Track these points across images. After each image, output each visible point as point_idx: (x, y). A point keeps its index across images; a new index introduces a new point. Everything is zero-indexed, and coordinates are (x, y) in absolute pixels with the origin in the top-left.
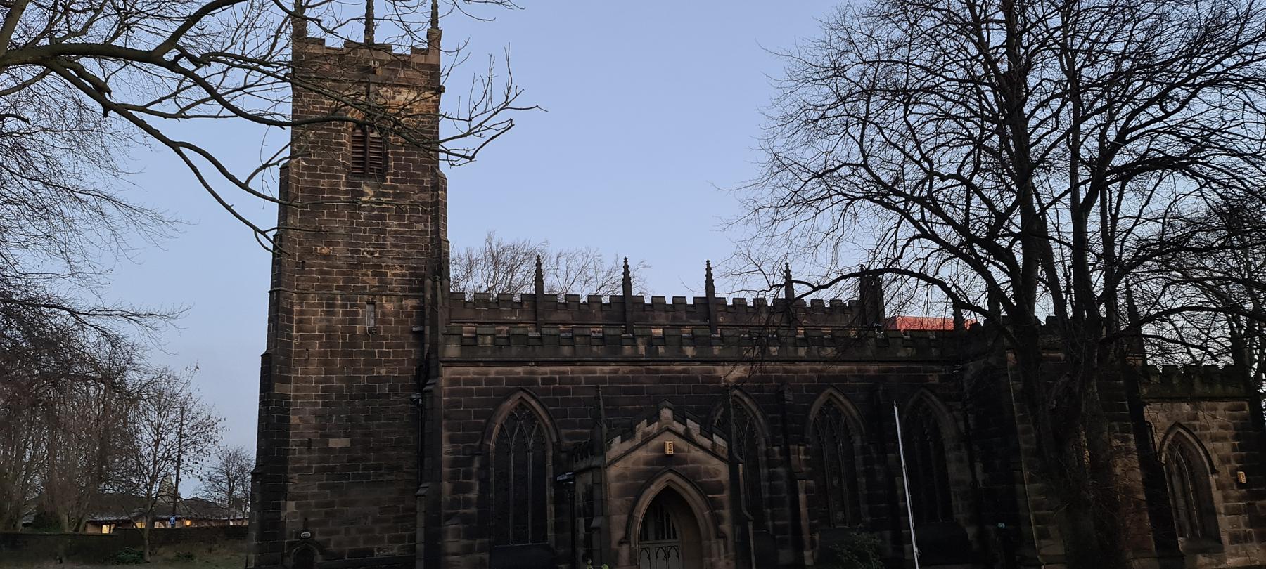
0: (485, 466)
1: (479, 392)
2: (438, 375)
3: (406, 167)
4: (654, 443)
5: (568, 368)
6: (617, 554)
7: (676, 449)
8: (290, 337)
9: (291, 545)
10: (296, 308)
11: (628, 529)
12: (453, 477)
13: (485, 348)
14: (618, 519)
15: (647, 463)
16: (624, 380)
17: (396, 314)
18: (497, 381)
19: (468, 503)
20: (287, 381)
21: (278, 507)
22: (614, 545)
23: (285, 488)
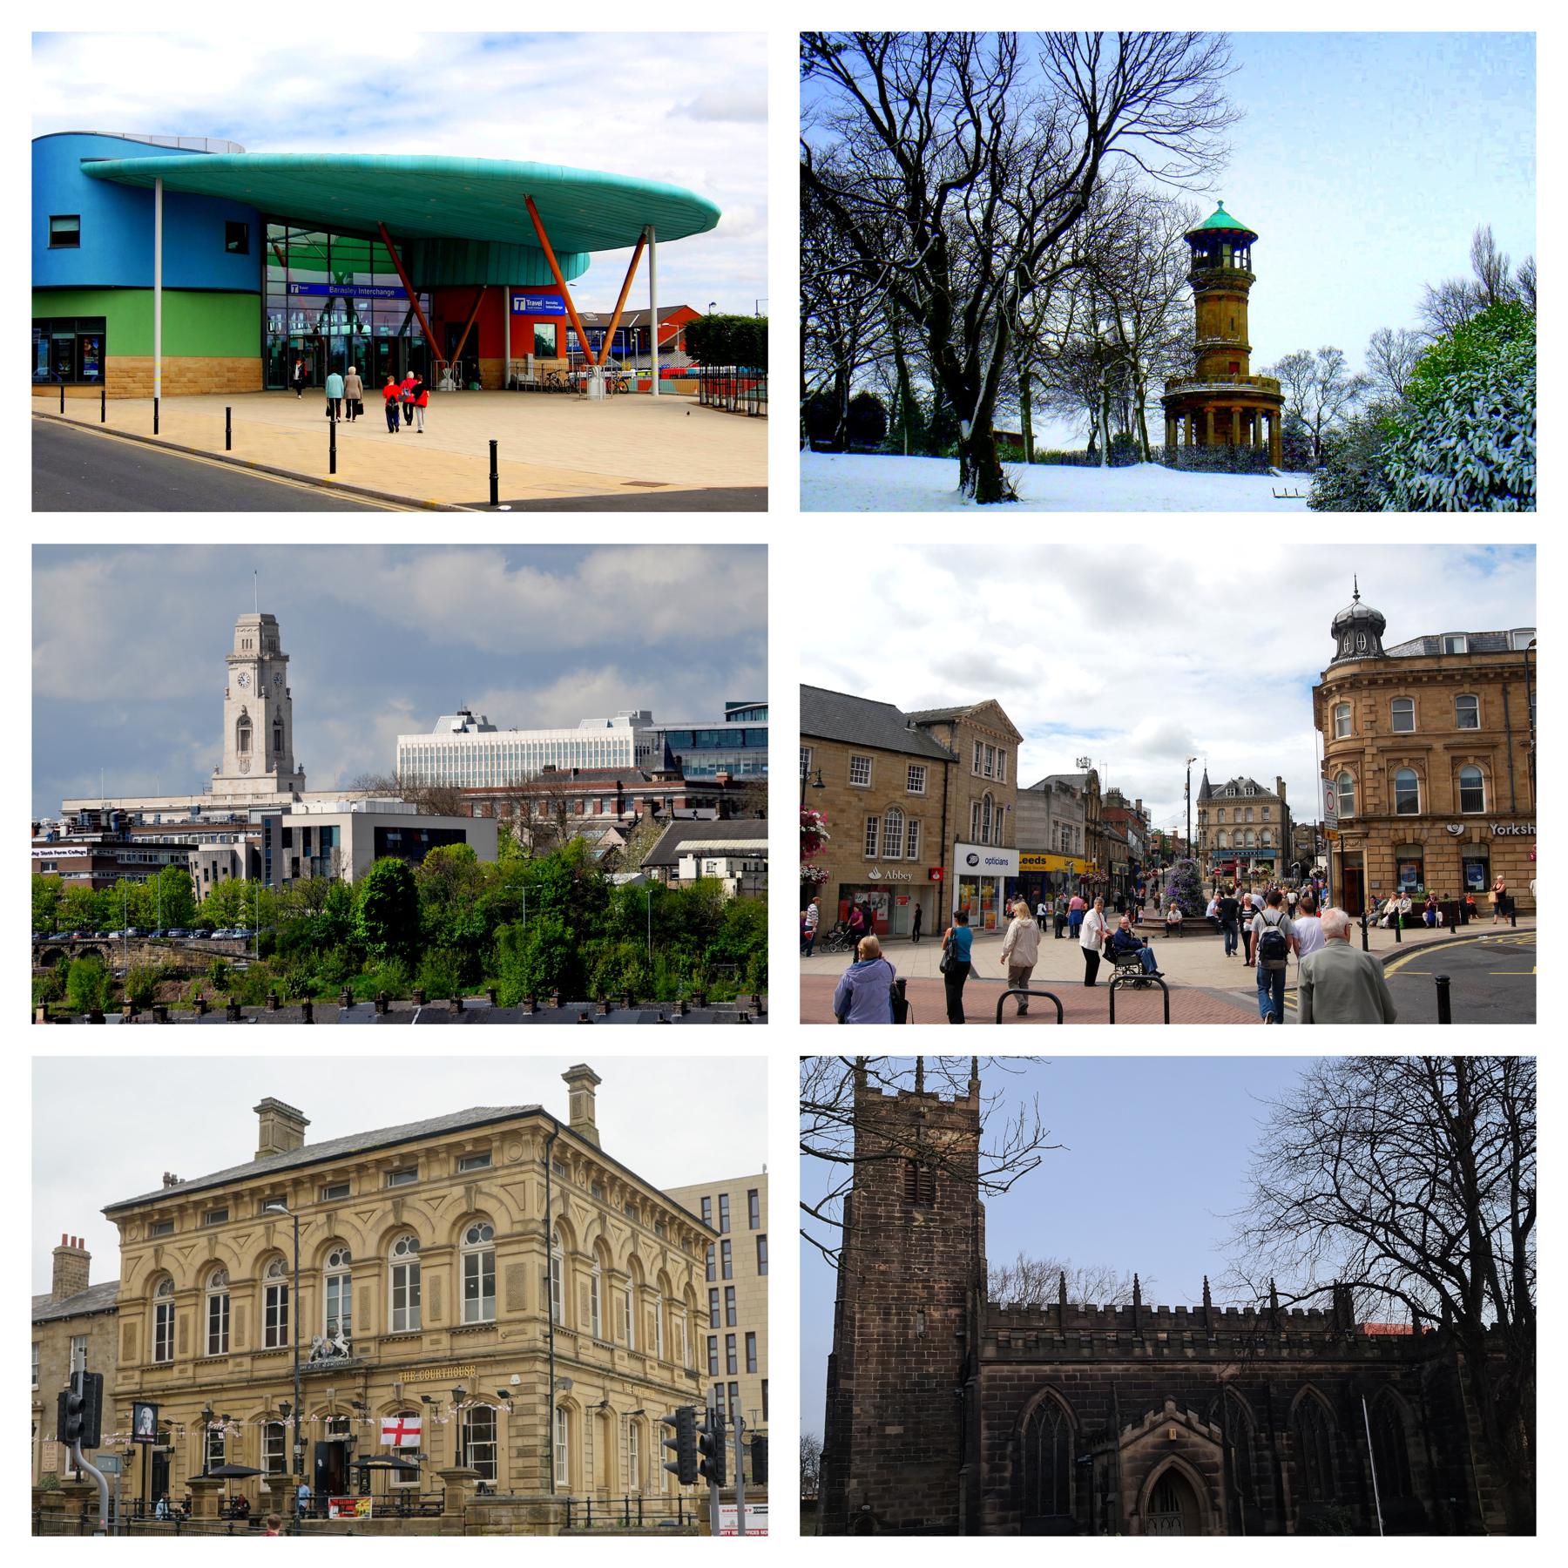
0: (1017, 1449)
1: (1012, 1387)
2: (977, 1373)
3: (951, 1197)
4: (1160, 1430)
5: (1087, 1367)
6: (1129, 1523)
7: (1179, 1435)
8: (853, 1341)
9: (854, 1516)
11: (1138, 1502)
12: (991, 1458)
13: (1017, 1350)
14: (1130, 1494)
15: (1154, 1447)
16: (1135, 1377)
17: (942, 1321)
18: (1027, 1378)
19: (1002, 1481)
20: (850, 1377)
21: (842, 1484)
22: (1126, 1517)
23: (848, 1468)
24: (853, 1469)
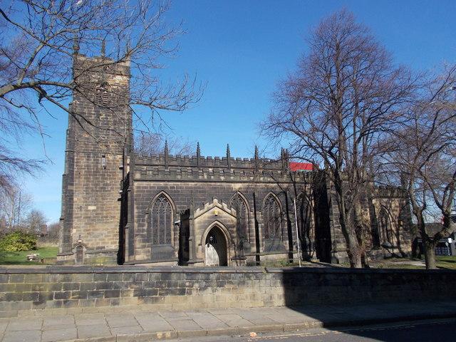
0: (149, 218)
2: (133, 185)
5: (179, 183)
7: (219, 213)
9: (75, 245)
10: (75, 158)
12: (139, 221)
15: (208, 218)
16: (199, 188)
17: (113, 161)
19: (143, 230)
20: (72, 185)
21: (69, 231)
22: (197, 245)
23: (72, 224)
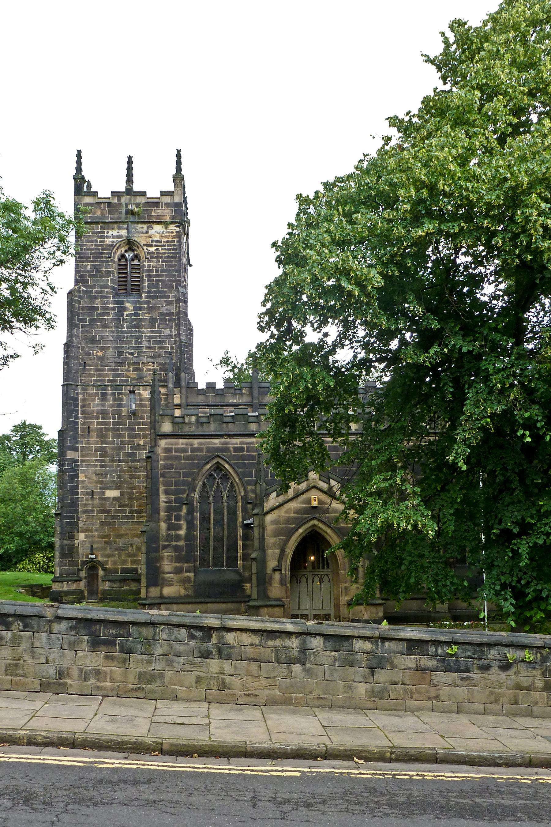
0: (190, 512)
1: (187, 458)
3: (156, 286)
4: (304, 496)
6: (271, 577)
7: (320, 502)
8: (77, 418)
9: (84, 563)
10: (80, 397)
11: (280, 560)
12: (168, 519)
13: (191, 425)
14: (273, 553)
15: (297, 512)
18: (200, 450)
19: (178, 538)
21: (72, 537)
22: (269, 571)
24: (81, 526)
